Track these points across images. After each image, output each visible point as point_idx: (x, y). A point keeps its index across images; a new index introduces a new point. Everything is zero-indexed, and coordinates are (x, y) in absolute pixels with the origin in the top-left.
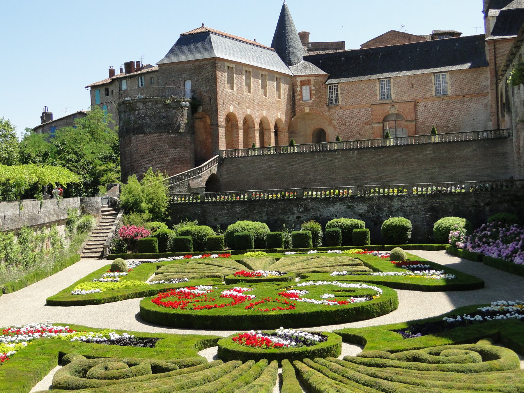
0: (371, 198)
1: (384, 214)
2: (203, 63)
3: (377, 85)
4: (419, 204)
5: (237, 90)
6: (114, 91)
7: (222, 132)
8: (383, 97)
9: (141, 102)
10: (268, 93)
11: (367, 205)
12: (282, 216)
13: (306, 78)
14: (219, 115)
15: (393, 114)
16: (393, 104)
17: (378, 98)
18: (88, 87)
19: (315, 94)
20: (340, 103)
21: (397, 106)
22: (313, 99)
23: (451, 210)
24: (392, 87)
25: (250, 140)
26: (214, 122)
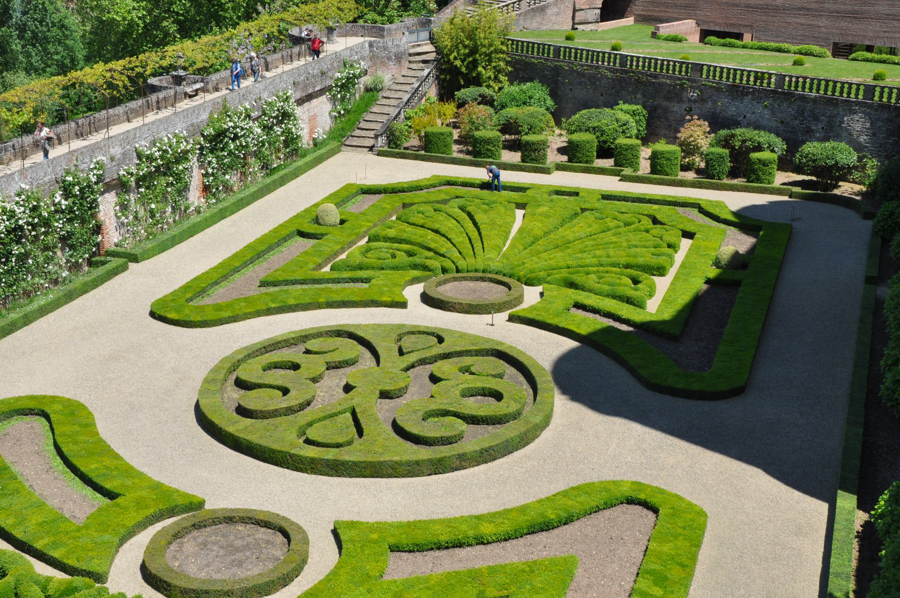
0: (803, 98)
1: (820, 127)
4: (878, 119)
11: (796, 108)
12: (665, 103)
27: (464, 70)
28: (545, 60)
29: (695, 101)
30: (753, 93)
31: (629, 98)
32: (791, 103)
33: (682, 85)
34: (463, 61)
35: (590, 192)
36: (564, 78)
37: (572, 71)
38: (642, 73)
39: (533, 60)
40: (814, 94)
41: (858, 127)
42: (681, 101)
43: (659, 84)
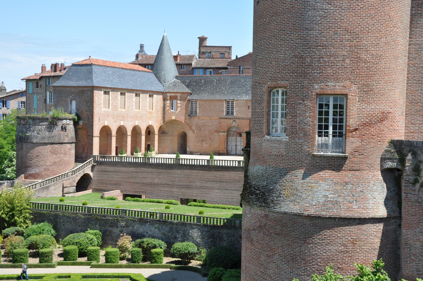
0: (171, 223)
1: (180, 236)
2: (84, 89)
3: (225, 104)
4: (204, 231)
5: (112, 109)
6: (42, 85)
7: (96, 142)
8: (228, 113)
9: (31, 119)
10: (141, 107)
11: (169, 227)
13: (174, 94)
14: (94, 129)
15: (234, 126)
16: (234, 119)
17: (225, 113)
18: (23, 79)
19: (180, 107)
21: (237, 121)
22: (179, 110)
23: (225, 239)
24: (234, 107)
25: (123, 143)
26: (90, 134)
27: (7, 219)
28: (50, 211)
29: (124, 227)
30: (150, 222)
31: (93, 227)
32: (167, 225)
33: (117, 220)
34: (6, 215)
35: (76, 275)
36: (60, 219)
37: (64, 216)
38: (98, 215)
39: (44, 212)
40: (176, 221)
41: (196, 235)
42: (117, 227)
43: (107, 220)
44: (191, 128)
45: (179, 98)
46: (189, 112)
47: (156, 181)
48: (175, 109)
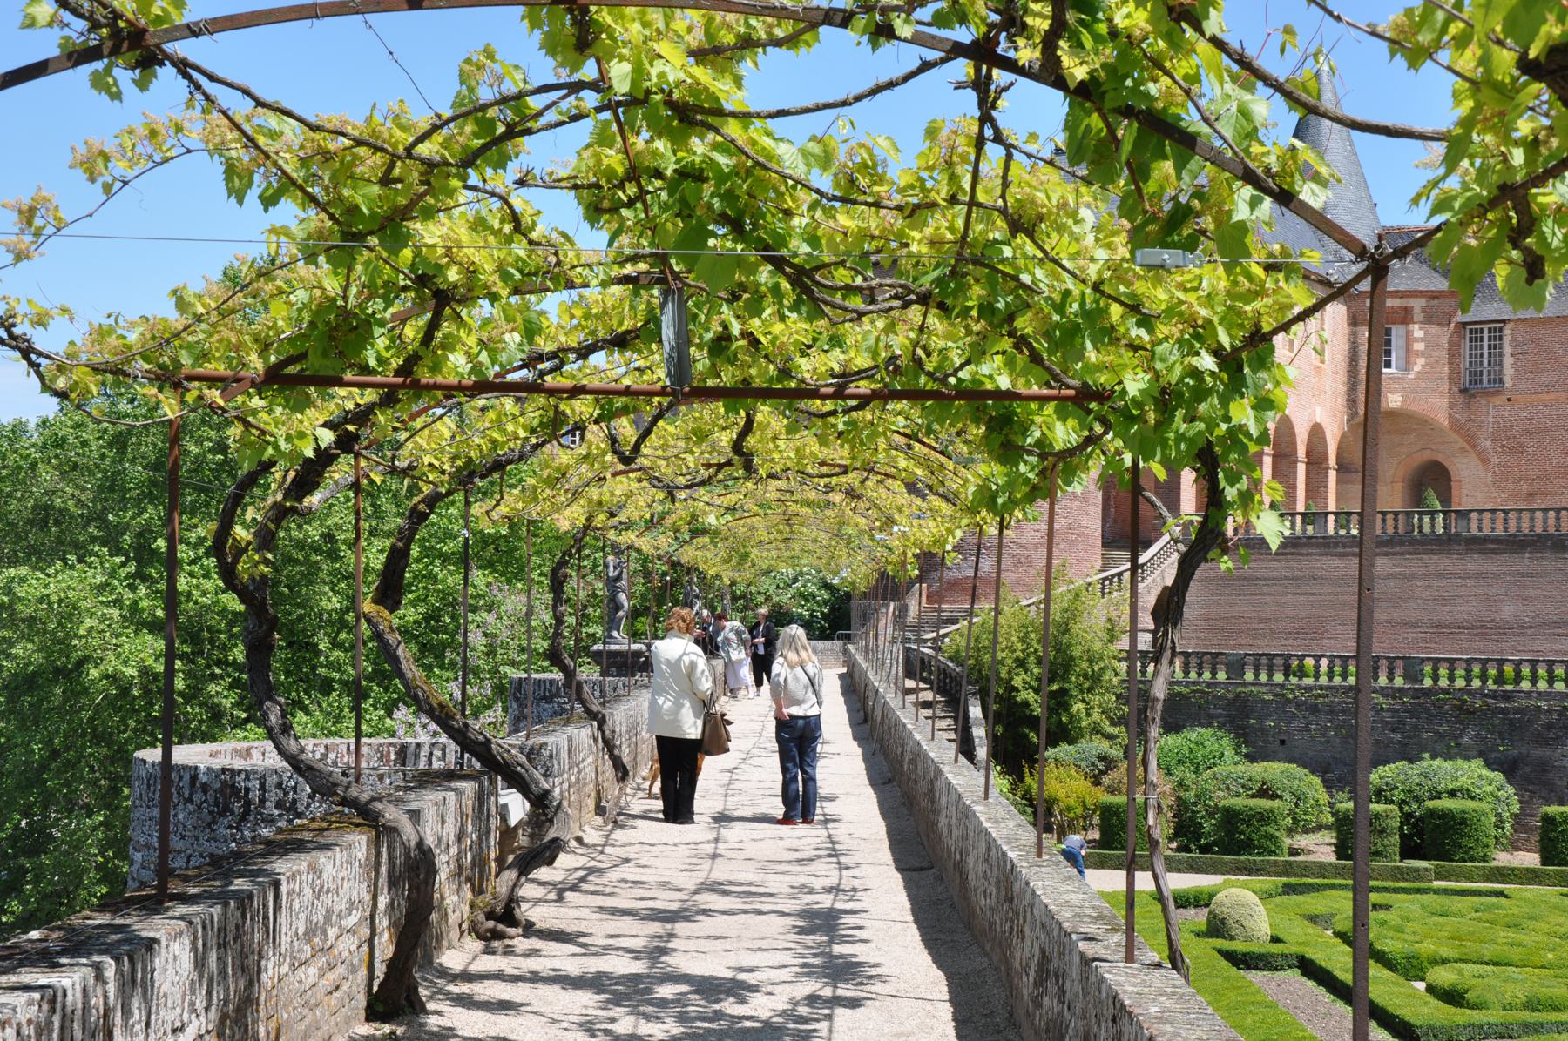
12: (1538, 752)
19: (1422, 354)
20: (1508, 384)
22: (1417, 368)
28: (1209, 685)
31: (1439, 747)
38: (1470, 693)
43: (1518, 711)
44: (1472, 441)
45: (1418, 315)
46: (1465, 379)
47: (1508, 611)
48: (1402, 363)
